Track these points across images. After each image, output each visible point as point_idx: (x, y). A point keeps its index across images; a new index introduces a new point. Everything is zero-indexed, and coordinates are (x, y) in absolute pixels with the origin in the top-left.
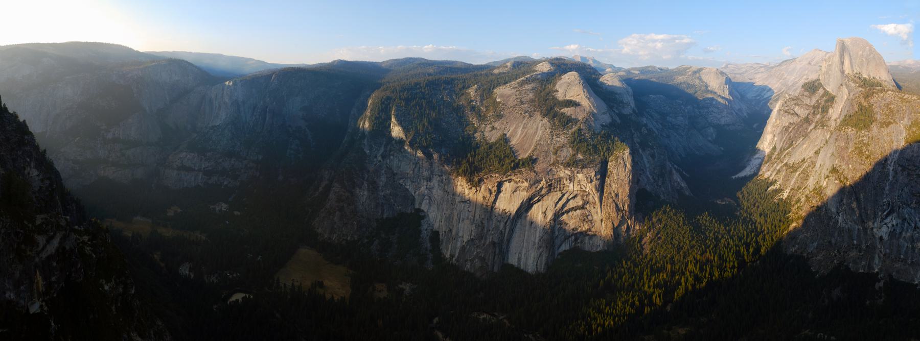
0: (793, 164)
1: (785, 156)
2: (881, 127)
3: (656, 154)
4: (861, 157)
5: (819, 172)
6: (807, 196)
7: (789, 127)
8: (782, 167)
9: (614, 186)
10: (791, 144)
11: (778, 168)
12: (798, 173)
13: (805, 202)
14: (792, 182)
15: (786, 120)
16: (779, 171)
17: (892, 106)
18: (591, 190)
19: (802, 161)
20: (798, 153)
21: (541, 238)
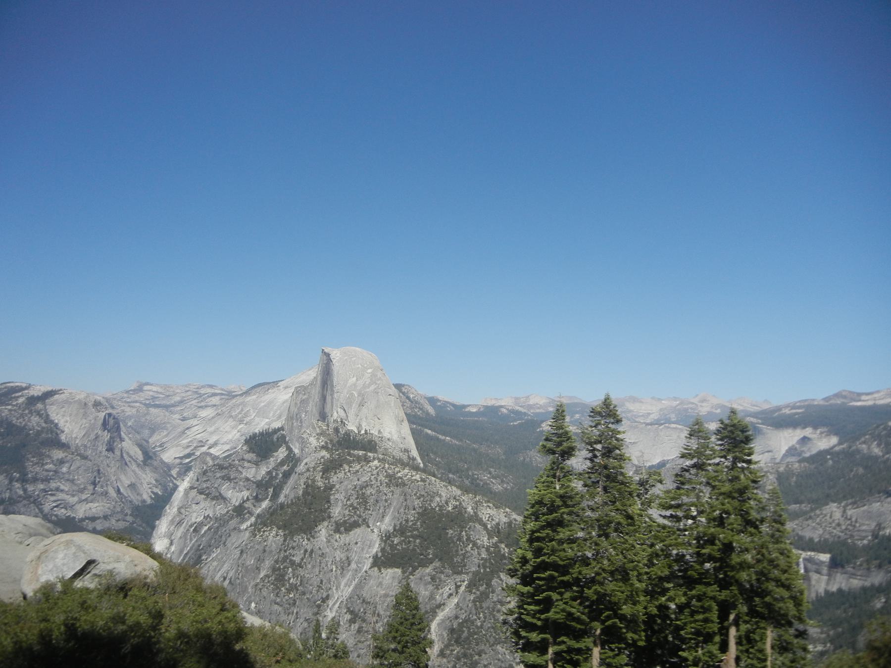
2: (335, 532)
4: (278, 588)
7: (201, 524)
17: (369, 491)
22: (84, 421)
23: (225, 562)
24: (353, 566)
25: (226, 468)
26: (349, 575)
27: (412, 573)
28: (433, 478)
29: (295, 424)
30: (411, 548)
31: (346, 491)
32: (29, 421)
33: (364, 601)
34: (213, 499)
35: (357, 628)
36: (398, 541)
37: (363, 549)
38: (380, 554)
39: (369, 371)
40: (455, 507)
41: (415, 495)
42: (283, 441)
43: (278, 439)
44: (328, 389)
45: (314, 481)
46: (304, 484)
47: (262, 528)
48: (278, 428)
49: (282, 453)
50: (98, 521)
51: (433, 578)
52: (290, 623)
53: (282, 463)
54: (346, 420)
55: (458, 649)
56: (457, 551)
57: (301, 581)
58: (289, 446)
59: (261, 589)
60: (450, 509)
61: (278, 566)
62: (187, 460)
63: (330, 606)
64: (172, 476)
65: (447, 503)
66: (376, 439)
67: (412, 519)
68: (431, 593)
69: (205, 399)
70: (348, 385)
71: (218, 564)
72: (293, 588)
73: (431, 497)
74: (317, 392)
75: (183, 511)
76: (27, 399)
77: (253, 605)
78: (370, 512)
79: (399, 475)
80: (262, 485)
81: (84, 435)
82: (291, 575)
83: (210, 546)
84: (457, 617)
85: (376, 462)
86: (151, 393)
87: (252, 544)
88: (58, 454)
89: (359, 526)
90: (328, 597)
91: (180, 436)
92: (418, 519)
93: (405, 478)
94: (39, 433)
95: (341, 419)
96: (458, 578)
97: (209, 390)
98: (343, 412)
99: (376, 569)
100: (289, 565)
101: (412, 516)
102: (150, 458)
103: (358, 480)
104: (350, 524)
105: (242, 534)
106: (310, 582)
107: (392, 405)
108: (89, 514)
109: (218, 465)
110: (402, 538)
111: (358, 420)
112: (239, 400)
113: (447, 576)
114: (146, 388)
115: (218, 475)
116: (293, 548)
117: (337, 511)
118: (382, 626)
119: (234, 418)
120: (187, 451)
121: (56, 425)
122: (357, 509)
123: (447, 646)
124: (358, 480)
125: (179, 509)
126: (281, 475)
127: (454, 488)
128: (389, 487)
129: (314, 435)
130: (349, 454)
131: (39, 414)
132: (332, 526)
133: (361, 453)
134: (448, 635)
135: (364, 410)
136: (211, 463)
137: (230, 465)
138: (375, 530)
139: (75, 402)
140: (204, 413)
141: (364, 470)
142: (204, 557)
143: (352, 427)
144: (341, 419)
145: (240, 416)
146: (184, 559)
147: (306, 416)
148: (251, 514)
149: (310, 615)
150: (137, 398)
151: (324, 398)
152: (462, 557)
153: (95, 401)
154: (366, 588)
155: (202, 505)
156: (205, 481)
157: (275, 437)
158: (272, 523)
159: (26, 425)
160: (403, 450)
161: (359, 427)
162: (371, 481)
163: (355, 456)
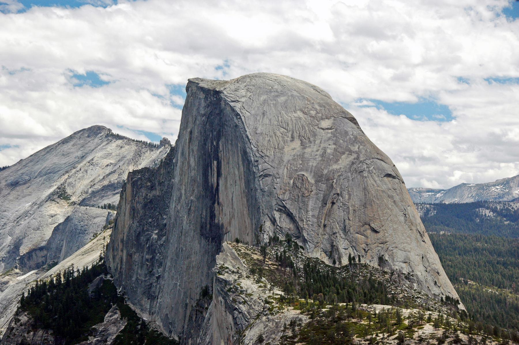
29: (136, 257)
39: (325, 124)
43: (98, 291)
44: (223, 172)
48: (94, 267)
54: (298, 237)
58: (127, 305)
70: (286, 159)
85: (428, 329)
95: (287, 235)
98: (288, 220)
111: (326, 237)
129: (244, 274)
130: (352, 313)
133: (379, 308)
135: (339, 213)
144: (287, 235)
147: (160, 236)
157: (91, 288)
160: (444, 299)
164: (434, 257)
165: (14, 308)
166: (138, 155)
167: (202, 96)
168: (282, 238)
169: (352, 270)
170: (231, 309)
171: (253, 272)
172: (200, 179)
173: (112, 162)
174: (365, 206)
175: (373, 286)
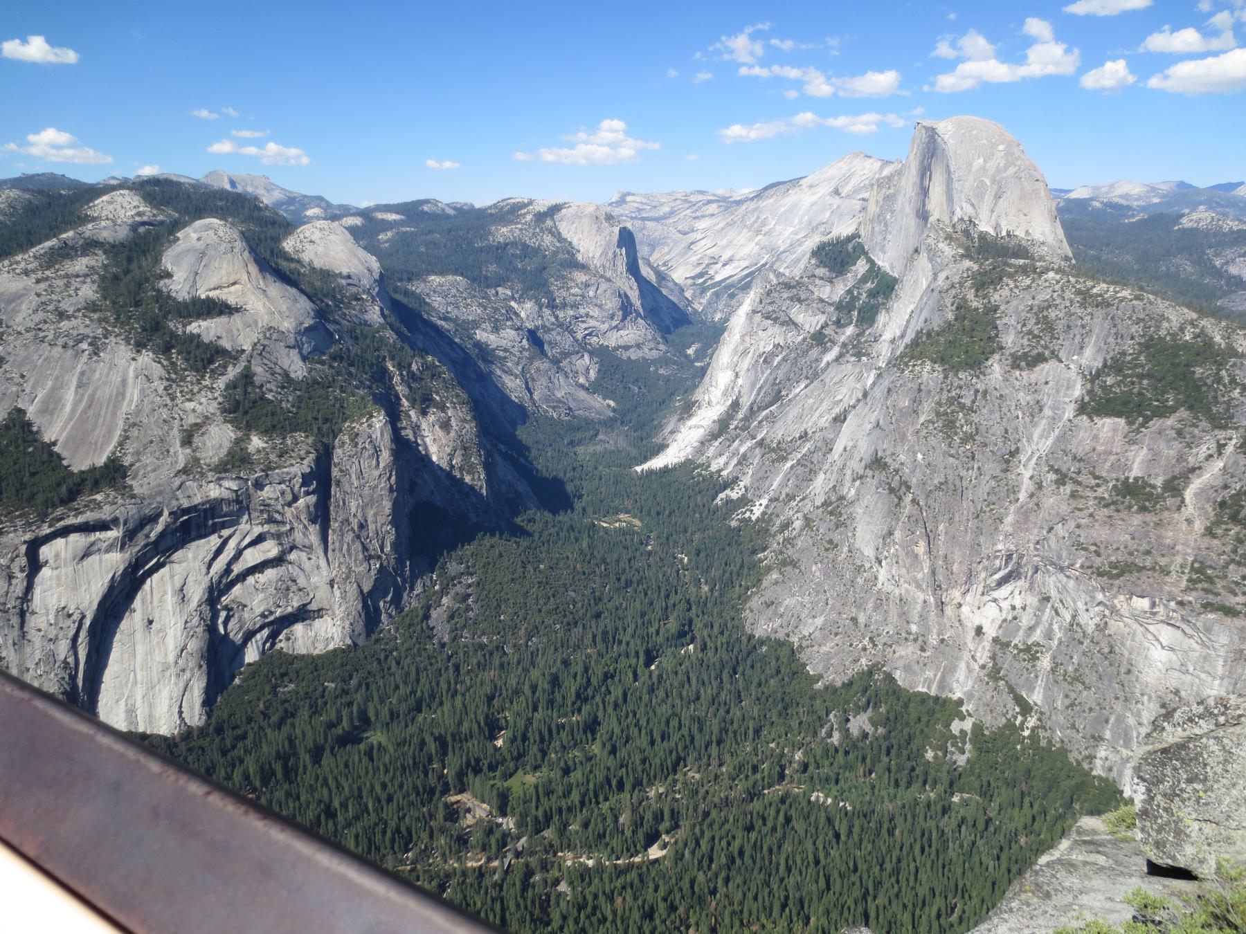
0: (779, 443)
1: (760, 422)
2: (1013, 368)
3: (453, 423)
5: (840, 463)
6: (806, 518)
7: (773, 354)
8: (751, 449)
9: (353, 505)
10: (777, 397)
11: (742, 450)
12: (789, 464)
13: (802, 530)
14: (775, 484)
15: (770, 337)
16: (744, 457)
17: (1053, 314)
18: (298, 518)
19: (801, 438)
20: (791, 416)
21: (182, 651)
22: (598, 238)
23: (822, 401)
24: (1047, 412)
25: (794, 287)
26: (1043, 424)
27: (1143, 425)
28: (1151, 297)
29: (877, 229)
30: (1135, 391)
31: (1017, 312)
32: (542, 240)
33: (1075, 457)
34: (782, 324)
35: (1068, 491)
36: (1112, 382)
37: (1058, 391)
38: (1087, 399)
39: (1001, 147)
40: (1196, 336)
41: (1130, 318)
42: (860, 251)
43: (854, 248)
45: (964, 299)
46: (952, 305)
47: (910, 361)
49: (861, 267)
50: (632, 350)
51: (1180, 433)
52: (971, 481)
53: (864, 279)
55: (1237, 529)
56: (1215, 397)
57: (977, 429)
59: (926, 438)
60: (1188, 338)
61: (942, 409)
62: (701, 281)
63: (1023, 460)
64: (687, 299)
65: (1182, 329)
66: (1023, 242)
67: (1131, 351)
68: (1179, 452)
69: (700, 208)
70: (974, 170)
71: (814, 403)
72: (968, 438)
73: (1157, 321)
74: (911, 183)
75: (747, 338)
76: (534, 215)
77: (920, 456)
78: (1059, 342)
79: (1095, 291)
80: (844, 307)
81: (601, 255)
82: (963, 421)
83: (789, 380)
84: (1226, 487)
85: (1051, 274)
86: (636, 205)
87: (901, 382)
88: (581, 277)
89: (1046, 360)
90: (1017, 451)
91: (686, 253)
92: (1140, 353)
93: (1106, 296)
94: (555, 253)
96: (1221, 435)
97: (700, 197)
98: (971, 208)
99: (1085, 417)
100: (958, 409)
101: (1129, 346)
102: (664, 279)
103: (1034, 298)
104: (1032, 357)
105: (844, 367)
106: (991, 431)
107: (1042, 193)
108: (621, 342)
109: (782, 283)
110: (1119, 378)
112: (752, 205)
113: (1204, 431)
114: (629, 199)
115: (785, 295)
116: (961, 388)
117: (1009, 340)
118: (1106, 490)
119: (750, 228)
120: (699, 270)
121: (570, 243)
122: (1041, 337)
123: (1217, 523)
124: (1034, 298)
125: (743, 337)
126: (865, 295)
127: (1186, 310)
128: (1085, 308)
130: (1006, 264)
131: (550, 232)
132: (1007, 360)
133: (1021, 262)
134: (1214, 509)
136: (775, 281)
137: (798, 283)
138: (1072, 366)
139: (586, 215)
140: (702, 225)
141: (1038, 285)
142: (783, 393)
143: (985, 227)
145: (756, 225)
146: (758, 394)
147: (892, 217)
148: (833, 342)
149: (997, 472)
150: (622, 212)
151: (924, 192)
152: (1224, 406)
153: (606, 214)
154: (1075, 441)
155: (770, 331)
156: (770, 303)
157: (850, 246)
158: (921, 356)
159: (540, 245)
161: (997, 227)
162: (1054, 300)
163: (1014, 266)
164: (1060, 232)
165: (808, 255)
166: (882, 168)
167: (924, 131)
168: (966, 218)
169: (1007, 239)
170: (931, 260)
171: (946, 239)
172: (918, 182)
173: (866, 172)
174: (1020, 199)
175: (1019, 249)
